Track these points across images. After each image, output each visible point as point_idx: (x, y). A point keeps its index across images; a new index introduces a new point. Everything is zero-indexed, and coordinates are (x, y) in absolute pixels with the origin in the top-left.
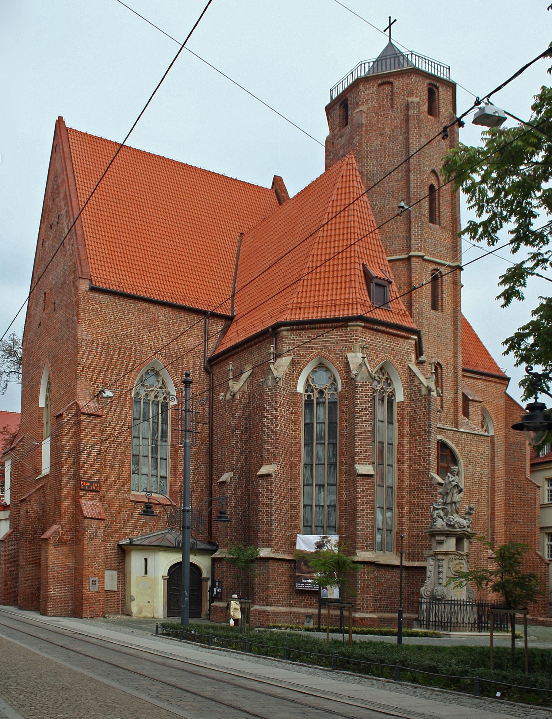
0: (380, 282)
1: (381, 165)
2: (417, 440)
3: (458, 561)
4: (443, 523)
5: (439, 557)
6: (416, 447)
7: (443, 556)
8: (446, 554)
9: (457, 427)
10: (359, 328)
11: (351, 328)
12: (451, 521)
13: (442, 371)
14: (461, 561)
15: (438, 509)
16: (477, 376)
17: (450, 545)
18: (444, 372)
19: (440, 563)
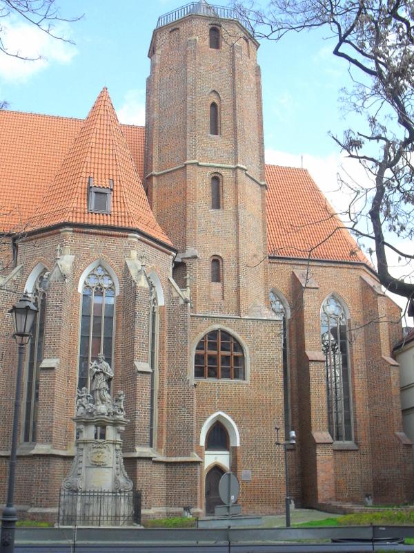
0: (98, 190)
3: (95, 450)
9: (240, 315)
10: (68, 233)
11: (63, 234)
14: (99, 450)
19: (80, 452)
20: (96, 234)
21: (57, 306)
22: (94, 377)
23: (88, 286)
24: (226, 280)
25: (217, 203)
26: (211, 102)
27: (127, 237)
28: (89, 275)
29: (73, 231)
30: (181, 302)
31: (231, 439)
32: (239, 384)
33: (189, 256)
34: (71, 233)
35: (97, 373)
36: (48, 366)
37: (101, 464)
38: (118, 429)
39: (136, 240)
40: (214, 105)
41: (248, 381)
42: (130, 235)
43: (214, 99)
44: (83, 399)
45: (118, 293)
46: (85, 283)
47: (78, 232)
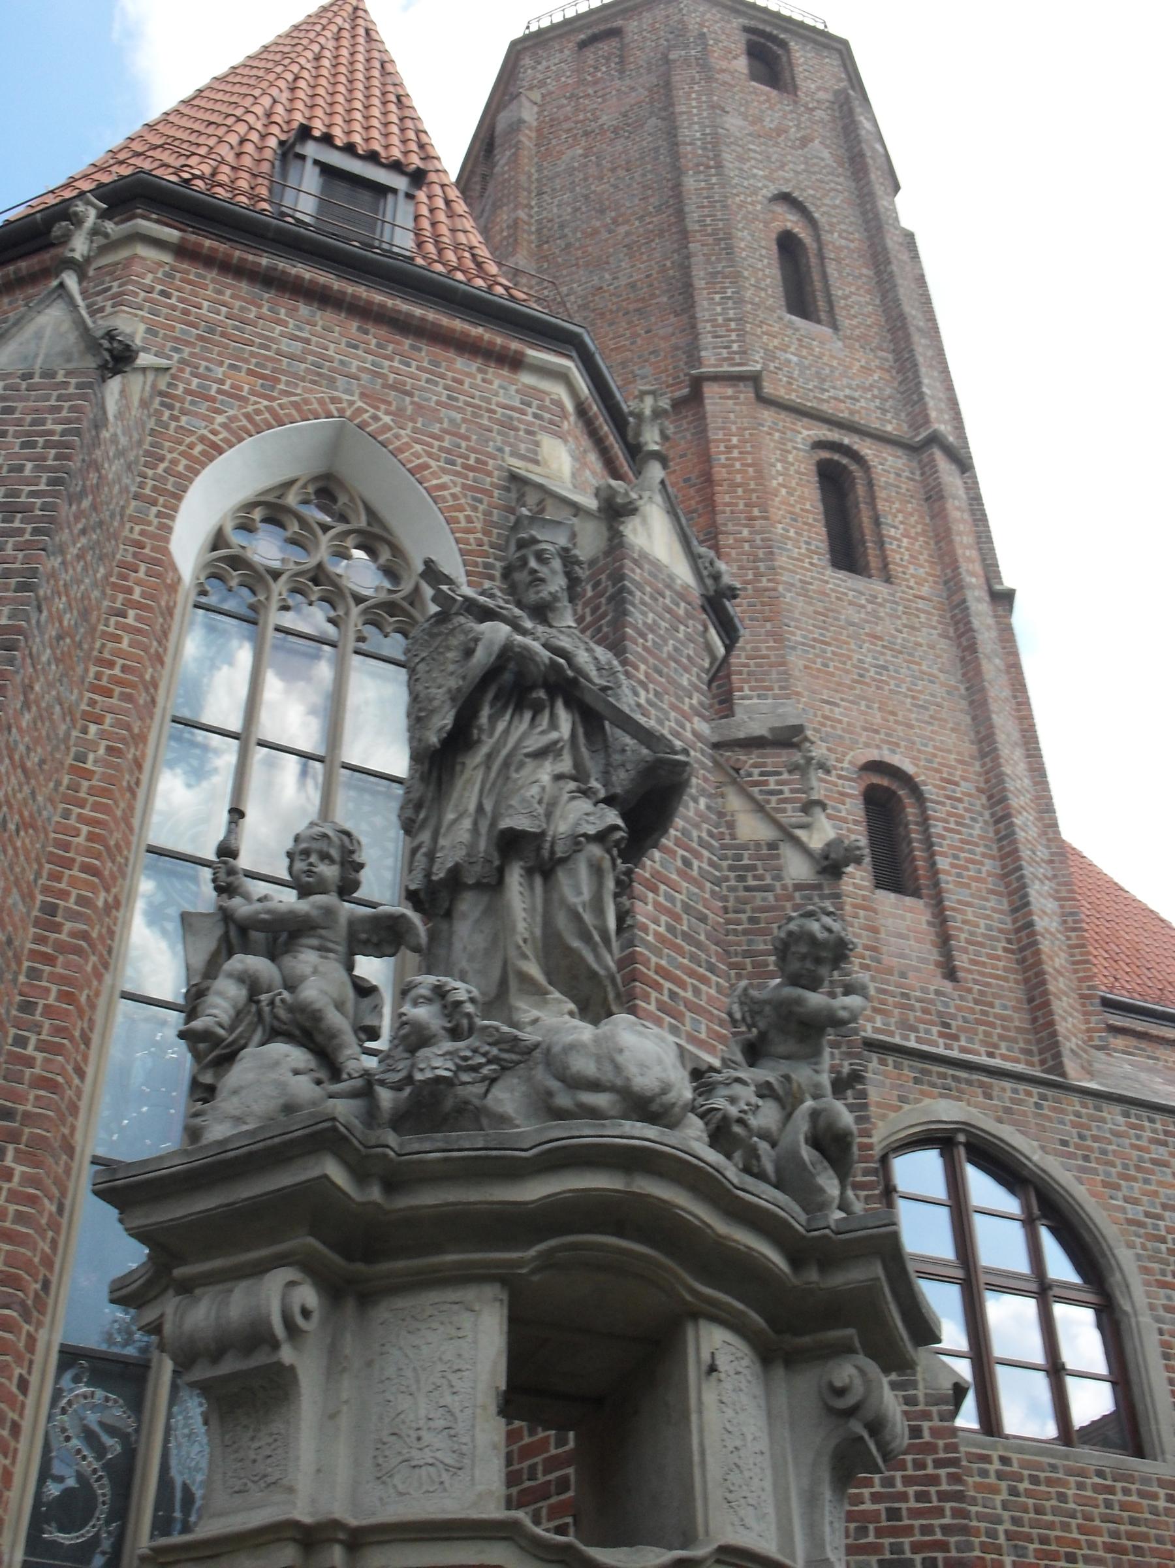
1: (586, 197)
10: (142, 250)
13: (923, 810)
18: (938, 812)
20: (322, 298)
23: (237, 562)
24: (948, 882)
25: (848, 549)
26: (777, 226)
27: (515, 363)
28: (250, 506)
29: (182, 251)
30: (797, 869)
32: (1130, 1479)
33: (758, 728)
34: (167, 258)
38: (841, 1409)
39: (569, 406)
40: (788, 244)
42: (532, 353)
43: (791, 221)
46: (218, 541)
47: (208, 261)
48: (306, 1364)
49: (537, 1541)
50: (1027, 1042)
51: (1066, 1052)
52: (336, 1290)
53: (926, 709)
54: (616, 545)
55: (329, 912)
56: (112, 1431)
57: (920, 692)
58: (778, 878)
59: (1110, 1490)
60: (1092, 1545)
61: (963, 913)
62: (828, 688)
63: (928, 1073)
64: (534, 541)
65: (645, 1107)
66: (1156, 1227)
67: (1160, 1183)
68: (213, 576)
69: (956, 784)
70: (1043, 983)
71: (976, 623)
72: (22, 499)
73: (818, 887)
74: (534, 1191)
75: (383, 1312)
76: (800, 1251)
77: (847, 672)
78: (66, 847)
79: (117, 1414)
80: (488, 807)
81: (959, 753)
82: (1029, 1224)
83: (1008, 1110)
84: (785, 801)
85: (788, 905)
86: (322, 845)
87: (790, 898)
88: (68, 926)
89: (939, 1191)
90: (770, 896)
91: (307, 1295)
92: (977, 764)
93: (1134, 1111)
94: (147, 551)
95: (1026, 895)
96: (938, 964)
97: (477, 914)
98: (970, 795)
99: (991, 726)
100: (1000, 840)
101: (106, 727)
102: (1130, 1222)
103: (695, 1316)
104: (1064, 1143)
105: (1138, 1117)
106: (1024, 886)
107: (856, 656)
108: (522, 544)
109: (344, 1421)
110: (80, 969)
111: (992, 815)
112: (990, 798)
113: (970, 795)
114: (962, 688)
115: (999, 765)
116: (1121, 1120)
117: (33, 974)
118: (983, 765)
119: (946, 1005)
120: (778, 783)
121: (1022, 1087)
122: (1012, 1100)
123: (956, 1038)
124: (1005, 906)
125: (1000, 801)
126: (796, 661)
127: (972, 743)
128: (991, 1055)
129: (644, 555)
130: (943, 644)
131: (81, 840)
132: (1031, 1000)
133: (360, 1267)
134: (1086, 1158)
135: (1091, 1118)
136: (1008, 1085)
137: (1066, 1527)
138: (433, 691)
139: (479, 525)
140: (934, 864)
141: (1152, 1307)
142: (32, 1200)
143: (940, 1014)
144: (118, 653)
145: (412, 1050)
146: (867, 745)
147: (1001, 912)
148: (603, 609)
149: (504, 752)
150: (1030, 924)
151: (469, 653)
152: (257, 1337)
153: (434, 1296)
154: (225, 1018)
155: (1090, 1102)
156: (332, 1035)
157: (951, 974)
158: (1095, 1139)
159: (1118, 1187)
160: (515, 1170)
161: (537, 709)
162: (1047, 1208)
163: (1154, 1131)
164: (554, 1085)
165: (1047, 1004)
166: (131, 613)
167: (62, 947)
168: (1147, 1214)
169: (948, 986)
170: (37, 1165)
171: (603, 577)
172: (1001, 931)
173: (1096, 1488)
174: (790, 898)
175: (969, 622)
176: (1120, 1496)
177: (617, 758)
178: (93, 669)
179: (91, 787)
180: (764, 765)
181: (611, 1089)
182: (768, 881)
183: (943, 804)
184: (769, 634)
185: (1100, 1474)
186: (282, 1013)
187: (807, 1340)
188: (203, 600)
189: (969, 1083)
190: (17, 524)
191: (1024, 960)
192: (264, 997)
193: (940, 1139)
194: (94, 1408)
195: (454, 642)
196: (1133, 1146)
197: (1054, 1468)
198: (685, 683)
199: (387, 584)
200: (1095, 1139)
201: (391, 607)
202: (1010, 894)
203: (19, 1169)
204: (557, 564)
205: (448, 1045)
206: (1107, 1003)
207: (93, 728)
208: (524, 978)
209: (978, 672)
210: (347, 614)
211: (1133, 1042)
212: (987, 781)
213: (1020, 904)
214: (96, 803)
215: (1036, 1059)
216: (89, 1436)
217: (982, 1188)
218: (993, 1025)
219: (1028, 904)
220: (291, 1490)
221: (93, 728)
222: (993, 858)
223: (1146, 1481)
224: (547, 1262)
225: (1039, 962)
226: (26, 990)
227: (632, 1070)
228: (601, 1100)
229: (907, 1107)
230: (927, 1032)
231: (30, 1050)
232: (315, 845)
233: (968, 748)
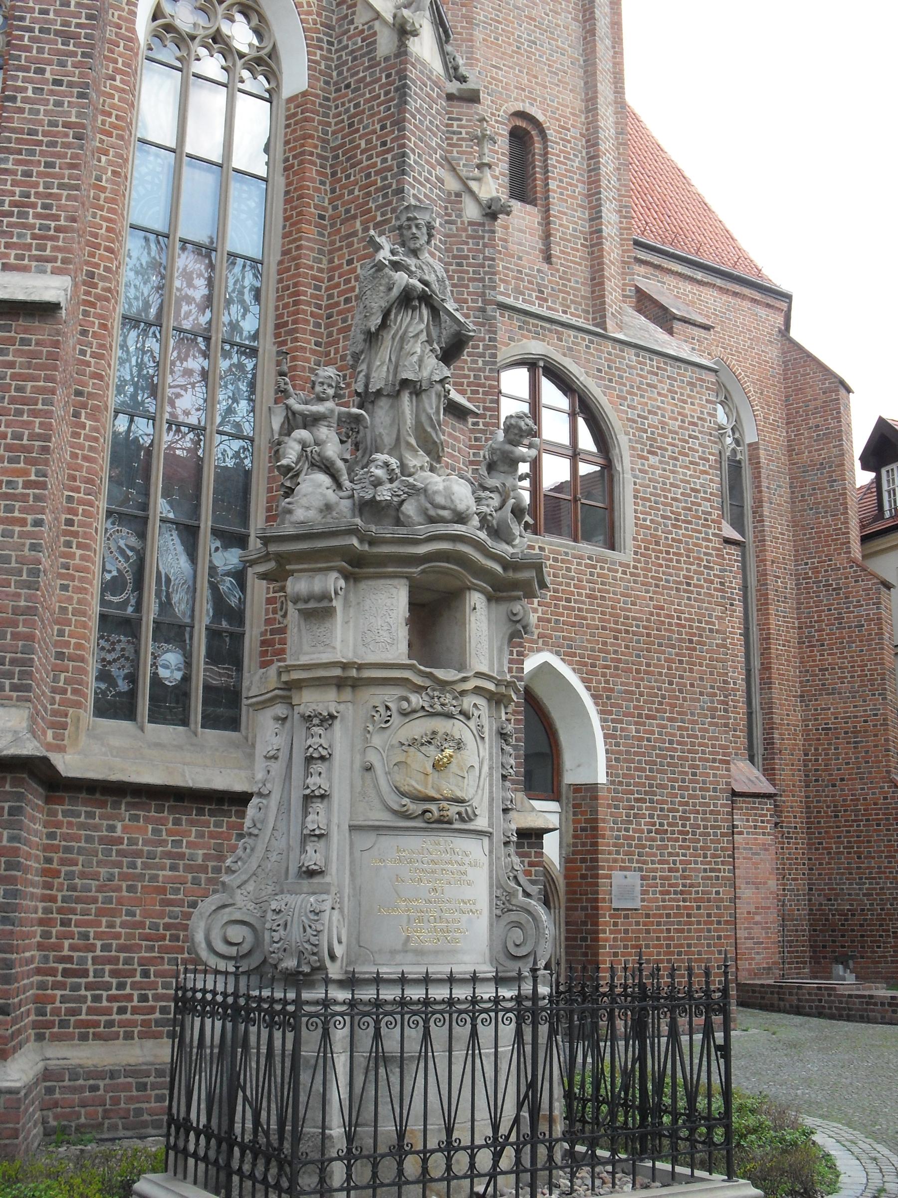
2: (354, 234)
3: (420, 727)
4: (332, 496)
5: (312, 701)
6: (350, 262)
7: (331, 694)
8: (349, 679)
12: (377, 483)
13: (546, 147)
14: (441, 725)
15: (311, 421)
16: (699, 276)
17: (375, 624)
18: (554, 149)
19: (319, 739)
21: (67, 37)
22: (386, 315)
23: (169, 28)
24: (554, 198)
30: (471, 211)
31: (569, 759)
35: (408, 299)
36: (21, 297)
37: (453, 810)
41: (626, 555)
44: (324, 432)
45: (296, 76)
48: (337, 604)
49: (420, 671)
50: (586, 305)
51: (609, 315)
52: (347, 577)
53: (557, 74)
54: (402, 51)
55: (332, 411)
56: (132, 549)
57: (554, 62)
58: (459, 216)
59: (595, 567)
60: (580, 594)
61: (561, 219)
62: (497, 56)
63: (528, 323)
64: (416, 219)
65: (461, 518)
66: (643, 424)
67: (650, 398)
68: (155, 36)
69: (568, 130)
70: (603, 270)
71: (598, 14)
72: (72, 29)
73: (483, 225)
74: (422, 550)
75: (363, 585)
76: (507, 565)
77: (510, 44)
78: (96, 236)
79: (133, 541)
80: (393, 359)
81: (573, 108)
82: (573, 416)
83: (570, 349)
84: (462, 139)
85: (464, 234)
86: (329, 381)
87: (466, 230)
88: (101, 284)
89: (525, 394)
90: (454, 227)
91: (342, 583)
92: (583, 116)
93: (642, 353)
94: (123, 31)
95: (601, 211)
96: (541, 251)
97: (387, 407)
98: (575, 138)
99: (596, 92)
100: (590, 171)
101: (110, 157)
102: (629, 420)
103: (469, 589)
104: (599, 371)
105: (643, 357)
106: (600, 205)
107: (517, 33)
108: (409, 219)
109: (351, 624)
110: (108, 309)
111: (587, 153)
112: (587, 141)
113: (575, 138)
114: (581, 59)
115: (597, 121)
116: (634, 358)
117: (86, 313)
118: (587, 118)
119: (543, 279)
120: (458, 126)
121: (580, 335)
122: (573, 343)
123: (546, 300)
124: (587, 216)
125: (593, 145)
126: (479, 35)
127: (582, 101)
128: (565, 312)
129: (418, 59)
130: (574, 26)
131: (103, 231)
132: (593, 279)
133: (357, 570)
134: (610, 381)
135: (617, 356)
136: (572, 333)
137: (568, 585)
138: (373, 304)
139: (314, 9)
140: (547, 184)
141: (633, 469)
142: (96, 440)
143: (538, 284)
144: (113, 106)
145: (375, 486)
146: (516, 100)
147: (583, 220)
148: (392, 94)
149: (400, 333)
150: (600, 231)
151: (390, 289)
152: (325, 597)
153: (382, 581)
154: (294, 460)
155: (618, 346)
156: (338, 471)
157: (548, 259)
158: (617, 369)
159: (625, 399)
160: (416, 542)
161: (414, 309)
162: (584, 407)
163: (652, 366)
164: (429, 506)
165: (602, 283)
166: (118, 77)
167: (99, 297)
168: (639, 416)
169: (545, 267)
170: (97, 421)
171: (393, 71)
172: (581, 232)
173: (586, 566)
174: (466, 230)
175: (593, 12)
176: (598, 570)
177: (443, 325)
178: (100, 118)
179: (106, 198)
180: (452, 112)
181: (450, 509)
182: (454, 218)
183: (558, 144)
184: (463, 16)
185: (590, 558)
186: (316, 457)
187: (505, 594)
188: (151, 54)
189: (550, 331)
190: (71, 48)
191: (593, 253)
192: (309, 449)
193: (531, 364)
194: (122, 538)
195: (383, 282)
196: (638, 375)
197: (566, 554)
198: (434, 145)
199: (256, 42)
200: (617, 369)
201: (259, 61)
202: (590, 208)
203: (88, 423)
204: (424, 230)
205: (389, 486)
206: (637, 243)
207: (103, 158)
208: (408, 444)
209: (594, 51)
210: (234, 65)
211: (651, 270)
212: (587, 130)
213: (596, 216)
214: (109, 208)
215: (590, 316)
216: (122, 552)
217: (550, 392)
218: (568, 293)
219: (601, 217)
220: (334, 648)
221: (103, 158)
222: (584, 183)
223: (614, 563)
224: (423, 571)
225: (602, 256)
226: (83, 323)
227: (458, 502)
228: (445, 513)
229: (513, 344)
230: (530, 295)
231: (88, 358)
232: (326, 381)
233: (579, 105)
